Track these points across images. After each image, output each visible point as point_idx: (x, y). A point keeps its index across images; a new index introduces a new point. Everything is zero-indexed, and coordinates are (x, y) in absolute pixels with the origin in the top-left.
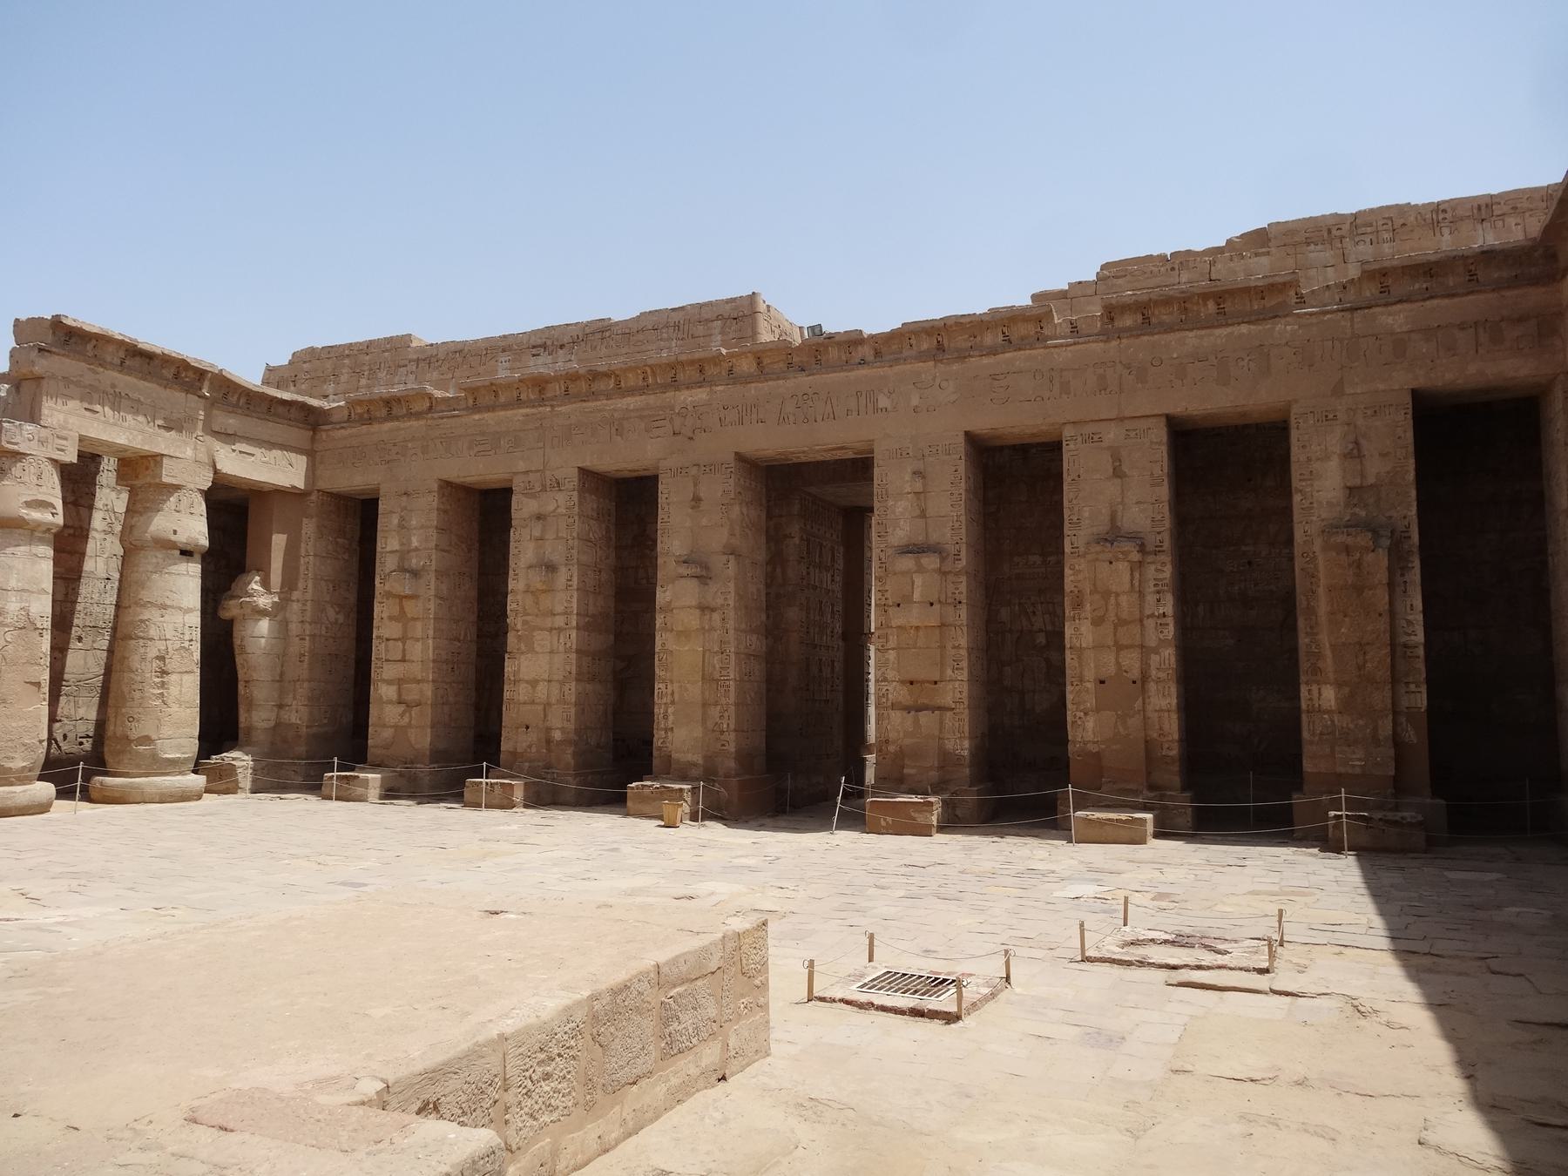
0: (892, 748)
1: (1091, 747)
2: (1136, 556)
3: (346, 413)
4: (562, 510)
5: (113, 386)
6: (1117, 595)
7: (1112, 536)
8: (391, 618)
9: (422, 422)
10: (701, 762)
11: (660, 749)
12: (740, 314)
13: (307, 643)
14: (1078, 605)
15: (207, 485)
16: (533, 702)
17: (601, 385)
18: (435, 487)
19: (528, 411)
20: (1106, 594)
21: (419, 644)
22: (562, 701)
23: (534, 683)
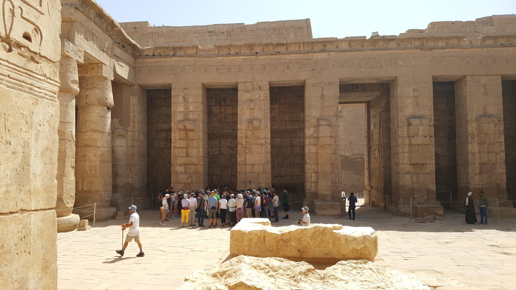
0: (406, 188)
1: (477, 186)
2: (497, 122)
3: (152, 52)
4: (262, 98)
5: (92, 29)
6: (490, 135)
7: (485, 115)
8: (180, 139)
9: (192, 59)
10: (330, 194)
11: (309, 190)
12: (305, 25)
13: (136, 149)
14: (473, 138)
15: (112, 78)
16: (252, 173)
17: (279, 49)
18: (201, 86)
19: (245, 57)
20: (486, 135)
21: (196, 150)
22: (264, 172)
23: (253, 165)
